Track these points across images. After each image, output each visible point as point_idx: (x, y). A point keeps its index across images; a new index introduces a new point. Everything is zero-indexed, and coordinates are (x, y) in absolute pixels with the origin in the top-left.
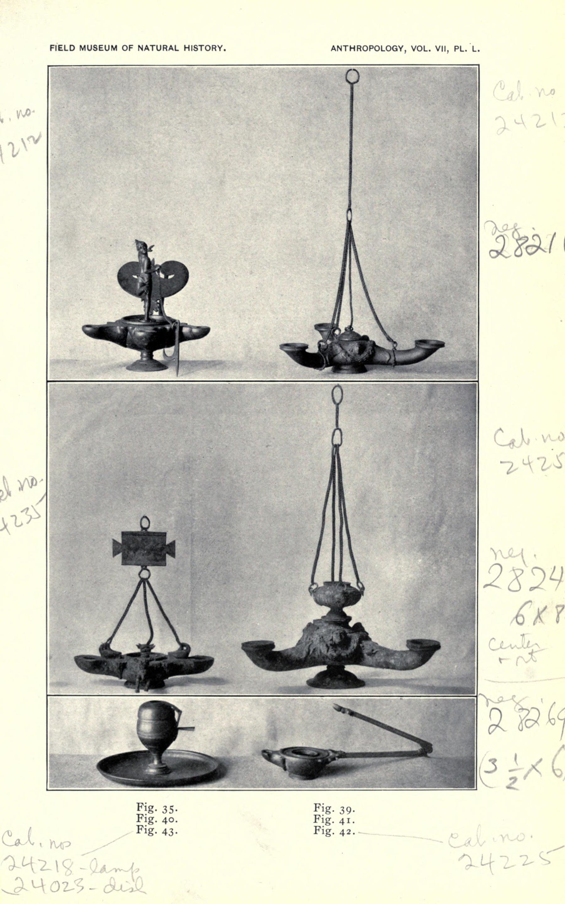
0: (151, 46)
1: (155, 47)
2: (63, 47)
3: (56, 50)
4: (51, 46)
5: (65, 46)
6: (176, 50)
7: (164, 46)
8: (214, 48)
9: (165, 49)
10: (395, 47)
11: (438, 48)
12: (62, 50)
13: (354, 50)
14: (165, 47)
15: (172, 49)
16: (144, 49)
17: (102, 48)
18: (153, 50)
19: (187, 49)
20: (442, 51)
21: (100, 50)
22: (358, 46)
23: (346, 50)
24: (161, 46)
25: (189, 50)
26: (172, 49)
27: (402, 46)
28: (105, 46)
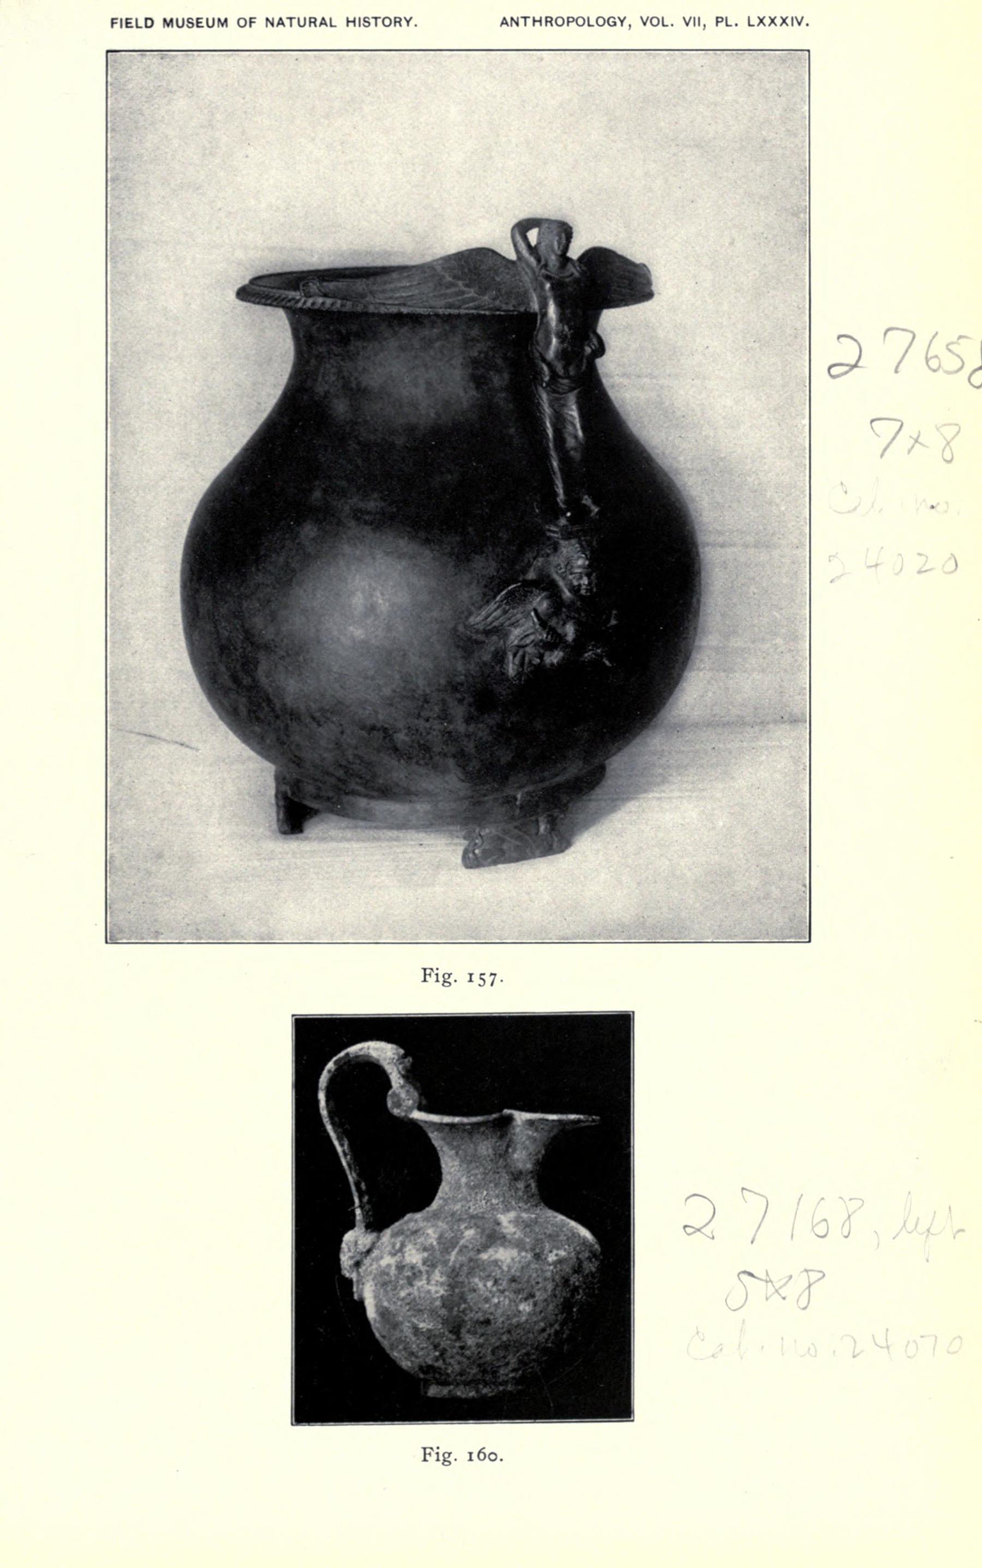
0: (288, 18)
1: (295, 22)
4: (113, 19)
5: (137, 20)
9: (312, 24)
11: (687, 20)
13: (541, 25)
14: (313, 20)
16: (276, 23)
18: (291, 26)
20: (694, 25)
21: (198, 26)
22: (546, 18)
24: (305, 19)
28: (207, 19)
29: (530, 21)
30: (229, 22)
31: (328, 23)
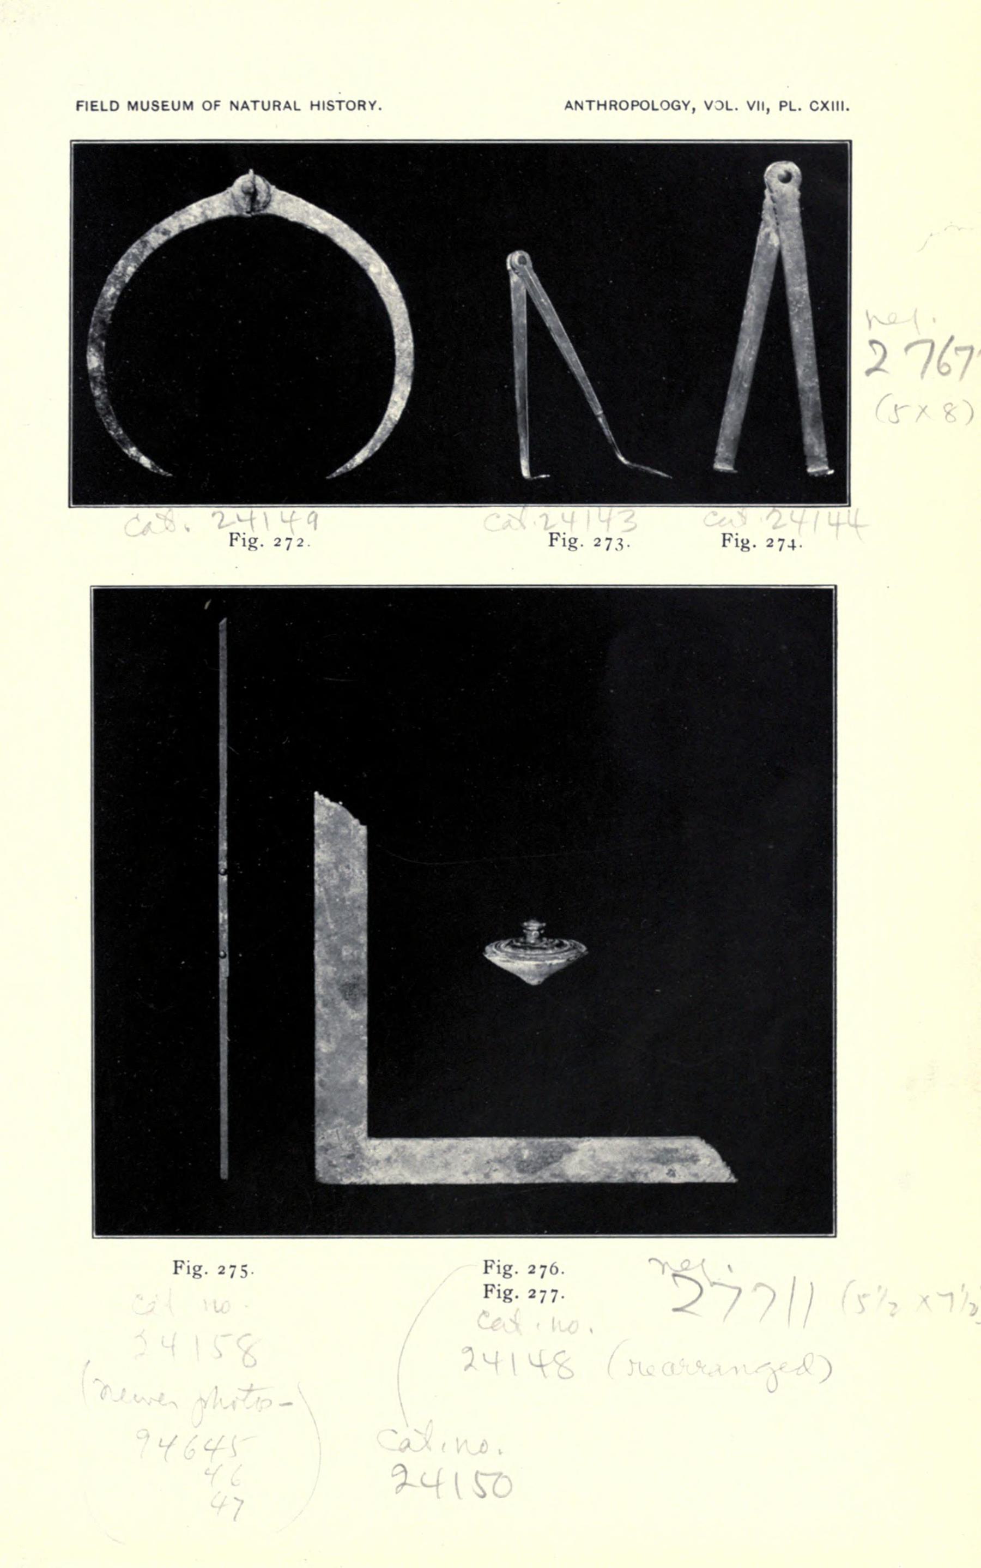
0: (252, 101)
1: (259, 105)
2: (99, 104)
3: (87, 109)
5: (102, 103)
6: (295, 109)
7: (274, 102)
8: (362, 104)
10: (676, 103)
11: (751, 104)
12: (97, 110)
13: (605, 109)
14: (277, 104)
15: (290, 107)
16: (240, 106)
17: (167, 106)
18: (255, 109)
19: (315, 108)
20: (758, 109)
21: (163, 109)
23: (590, 109)
24: (269, 102)
25: (319, 109)
26: (290, 107)
27: (689, 102)
28: (173, 103)
29: (594, 105)
30: (194, 105)
31: (292, 105)
